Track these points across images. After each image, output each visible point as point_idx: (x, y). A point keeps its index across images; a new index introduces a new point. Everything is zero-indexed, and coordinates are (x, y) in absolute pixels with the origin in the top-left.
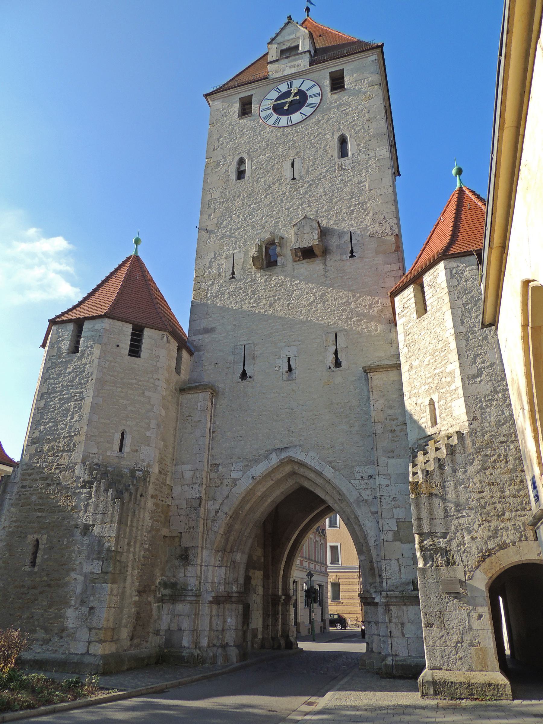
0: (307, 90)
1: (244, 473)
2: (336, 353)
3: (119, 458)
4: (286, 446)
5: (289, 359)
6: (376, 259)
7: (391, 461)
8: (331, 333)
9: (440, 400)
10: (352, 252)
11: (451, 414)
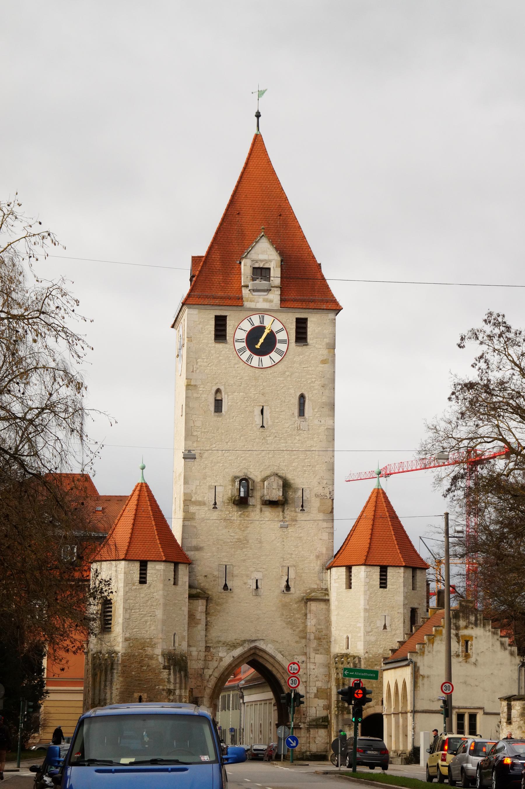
1: (227, 654)
2: (287, 581)
3: (175, 650)
4: (254, 639)
5: (257, 580)
6: (318, 516)
7: (317, 655)
8: (285, 566)
9: (352, 638)
10: (302, 506)
11: (356, 647)
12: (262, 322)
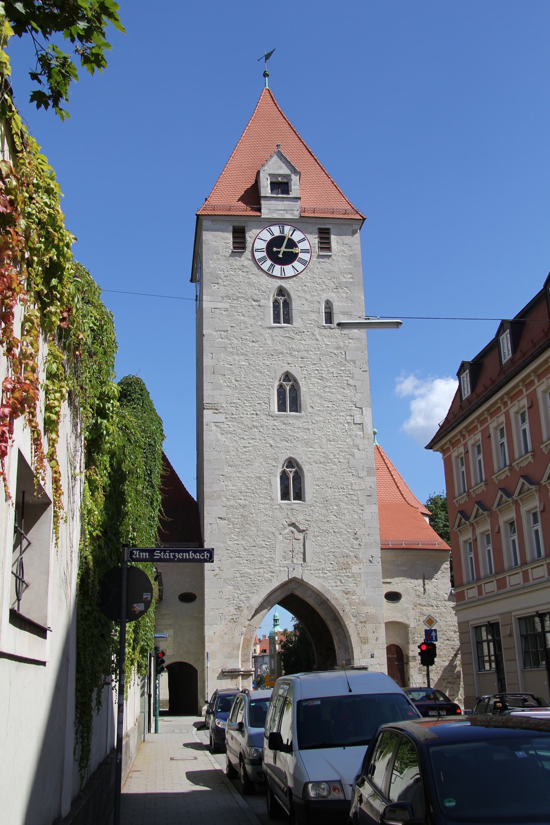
0: (300, 241)
12: (282, 232)
